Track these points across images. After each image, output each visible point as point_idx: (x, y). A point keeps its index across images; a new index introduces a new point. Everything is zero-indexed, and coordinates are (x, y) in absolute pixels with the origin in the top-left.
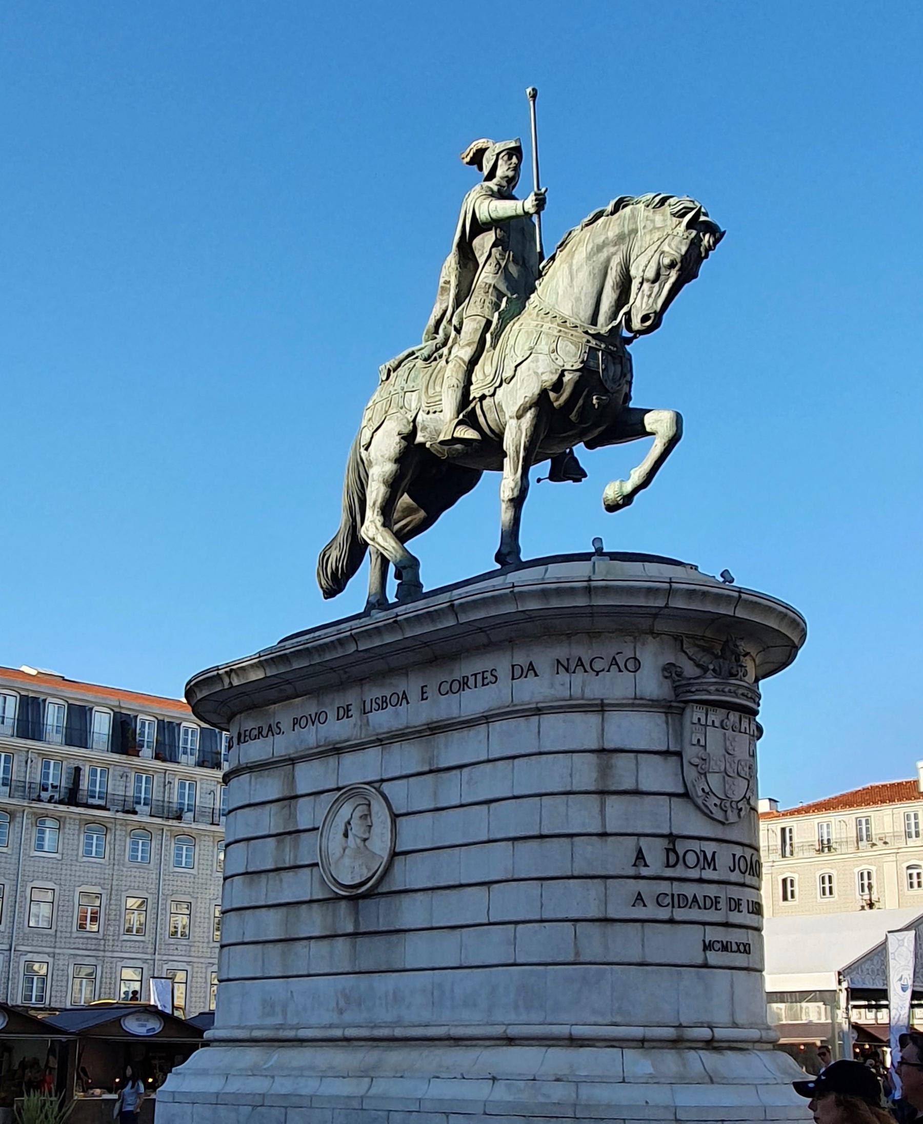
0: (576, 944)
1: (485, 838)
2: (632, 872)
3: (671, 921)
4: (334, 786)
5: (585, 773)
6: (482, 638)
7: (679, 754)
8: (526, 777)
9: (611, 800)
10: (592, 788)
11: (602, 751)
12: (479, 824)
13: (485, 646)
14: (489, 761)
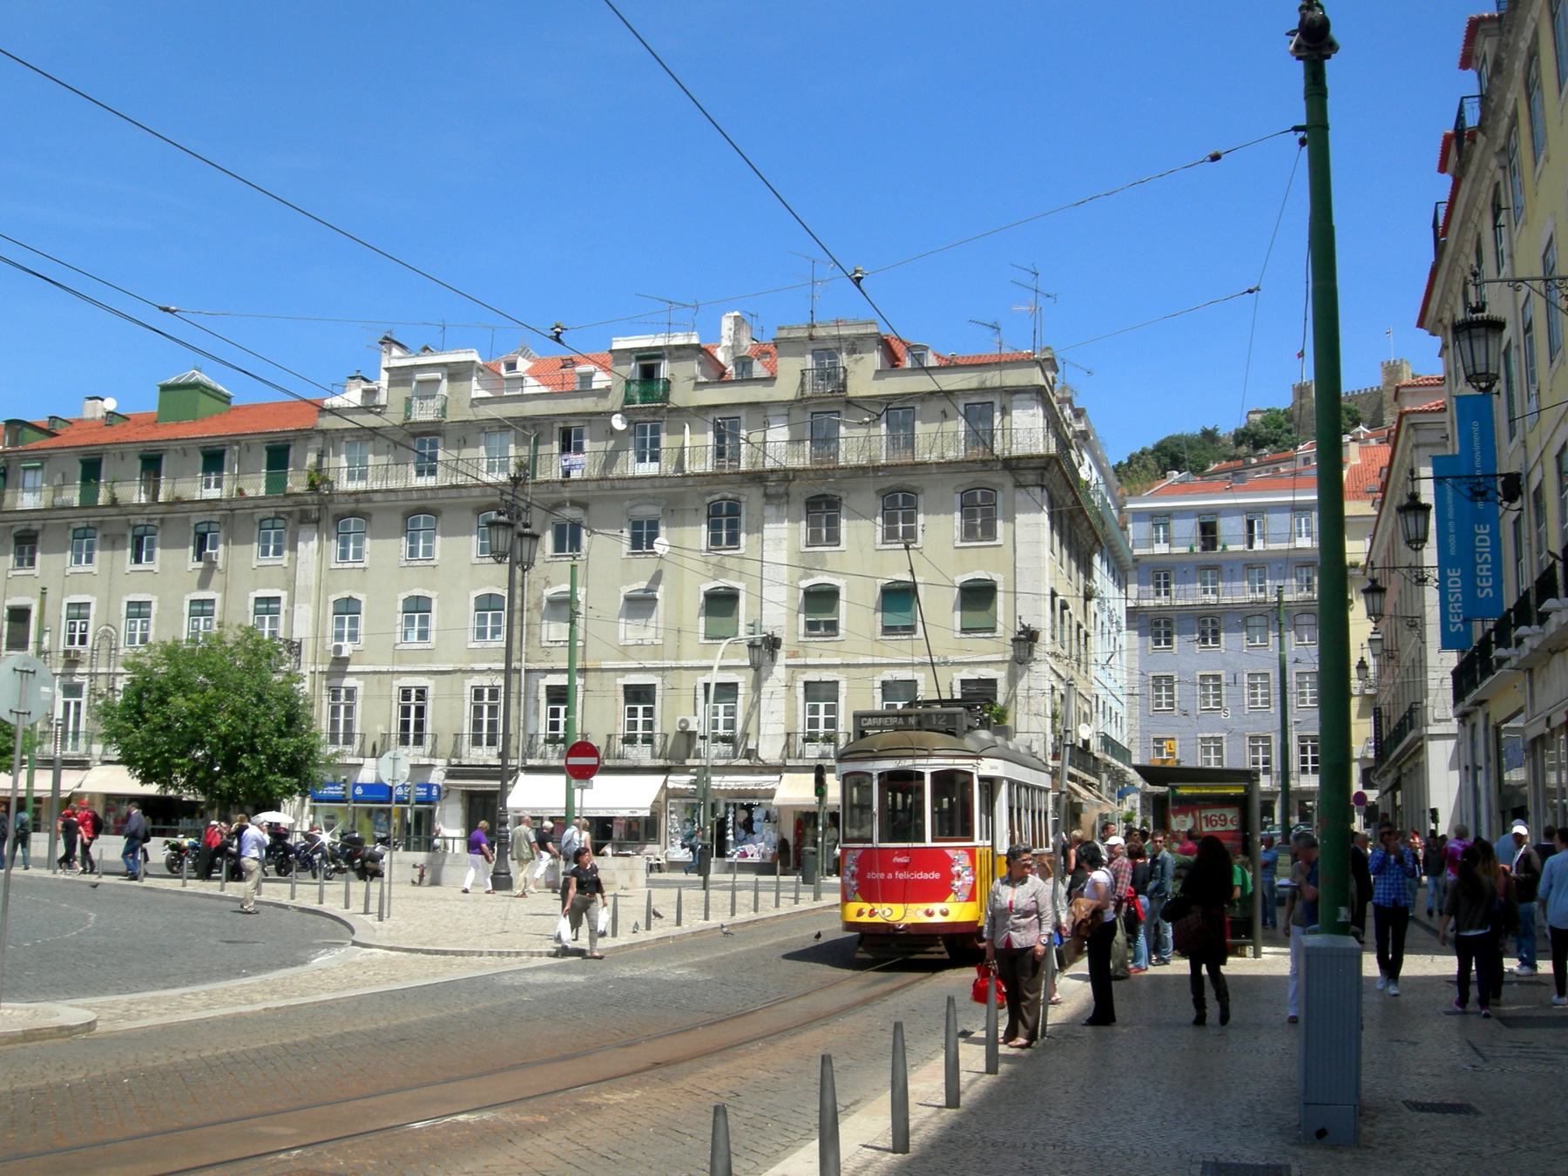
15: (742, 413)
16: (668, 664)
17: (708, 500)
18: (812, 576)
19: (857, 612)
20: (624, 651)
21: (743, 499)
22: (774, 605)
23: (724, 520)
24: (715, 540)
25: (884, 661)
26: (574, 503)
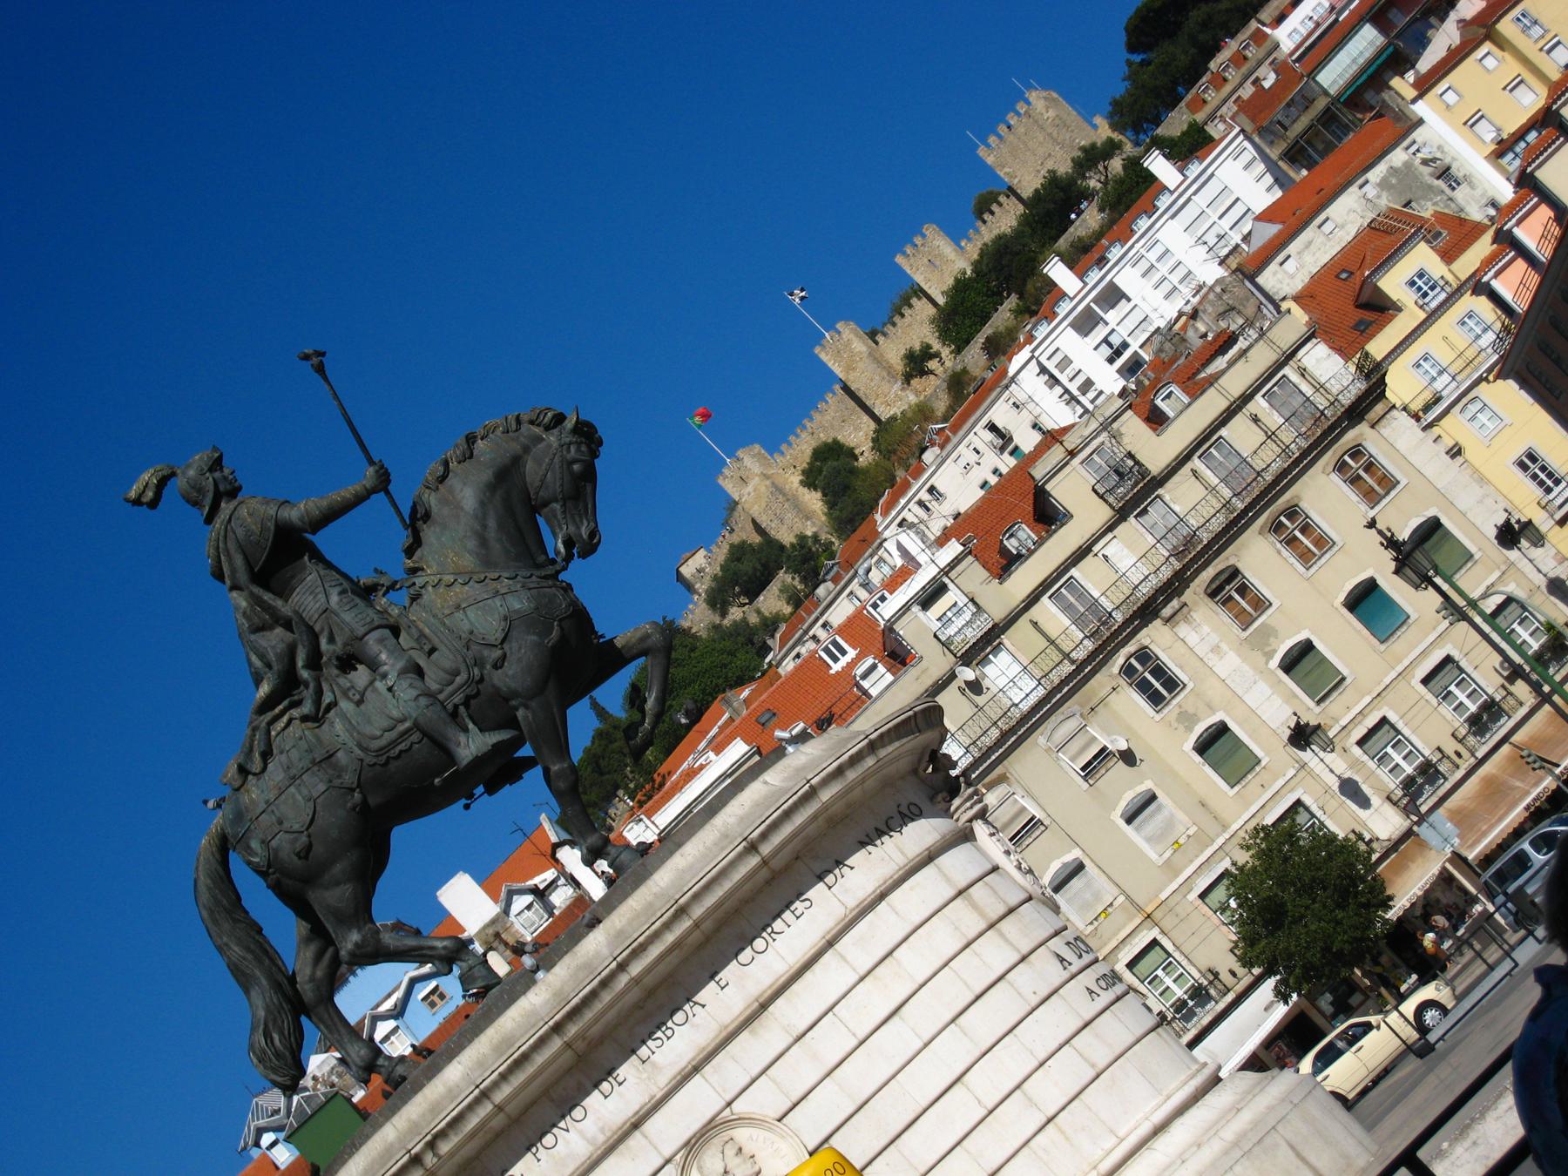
0: (1086, 1060)
1: (920, 1044)
2: (1066, 975)
3: (1118, 999)
4: (660, 1162)
5: (965, 919)
6: (765, 873)
7: (995, 869)
8: (915, 961)
9: (1003, 925)
10: (983, 925)
11: (960, 893)
12: (898, 1040)
13: (768, 882)
14: (862, 979)
15: (1074, 572)
16: (1220, 841)
17: (1116, 670)
18: (1275, 651)
19: (1343, 640)
20: (1170, 868)
21: (1146, 642)
22: (1264, 706)
23: (1147, 675)
24: (1156, 699)
25: (1406, 662)
26: (990, 787)
